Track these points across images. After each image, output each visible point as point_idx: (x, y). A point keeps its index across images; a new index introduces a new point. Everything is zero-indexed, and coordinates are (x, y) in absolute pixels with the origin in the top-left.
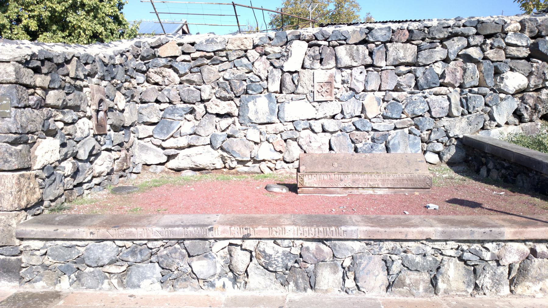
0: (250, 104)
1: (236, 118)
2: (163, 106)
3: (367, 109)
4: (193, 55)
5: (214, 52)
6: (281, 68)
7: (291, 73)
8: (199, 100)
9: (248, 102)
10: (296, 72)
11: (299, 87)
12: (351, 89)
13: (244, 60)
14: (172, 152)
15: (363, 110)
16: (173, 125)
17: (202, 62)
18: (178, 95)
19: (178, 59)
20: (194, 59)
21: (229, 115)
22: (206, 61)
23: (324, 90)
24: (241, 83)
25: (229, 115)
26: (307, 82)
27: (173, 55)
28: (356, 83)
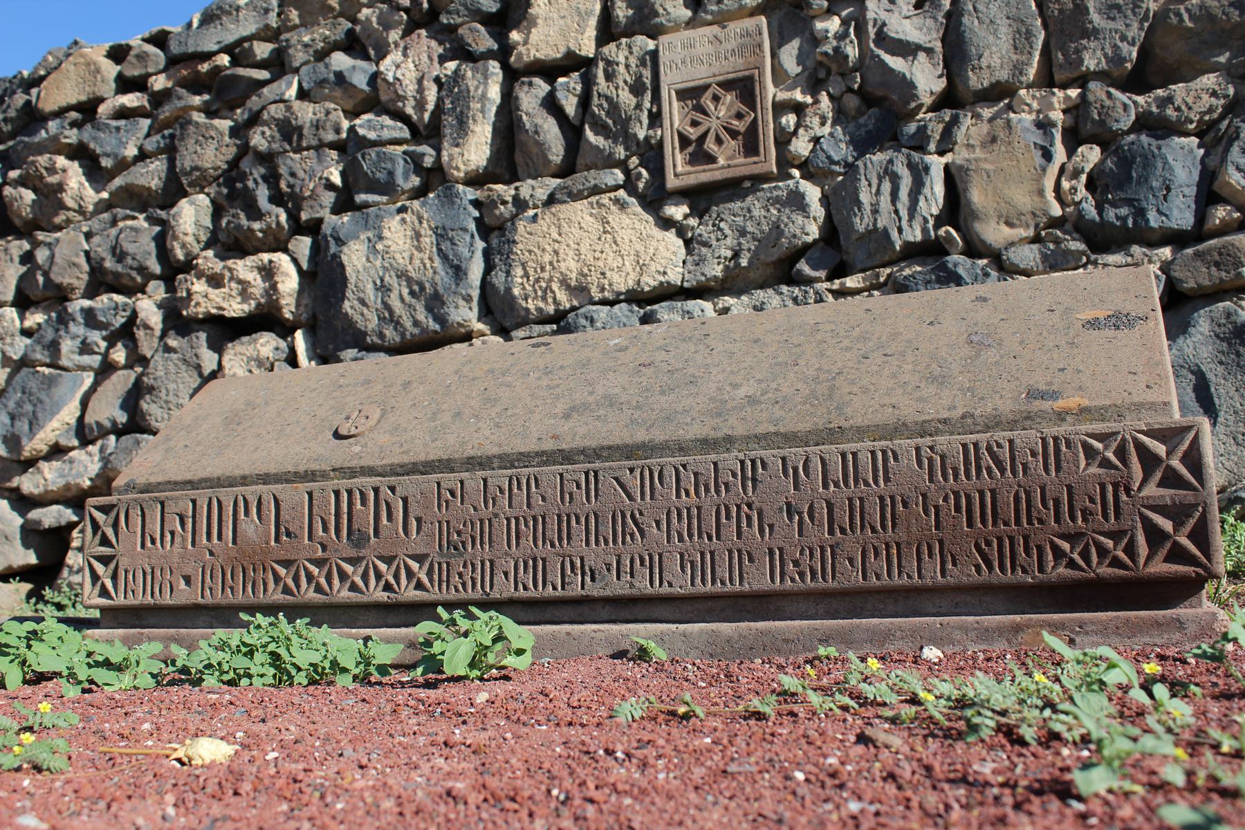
0: (354, 257)
1: (299, 335)
2: (36, 318)
3: (977, 196)
4: (159, 83)
5: (228, 50)
6: (504, 53)
7: (549, 71)
8: (157, 269)
9: (340, 242)
10: (572, 63)
11: (589, 134)
12: (867, 98)
13: (340, 60)
14: (51, 516)
15: (955, 208)
16: (59, 391)
17: (180, 104)
18: (82, 261)
19: (102, 109)
20: (159, 99)
21: (265, 319)
22: (197, 100)
23: (714, 124)
24: (320, 159)
25: (265, 319)
26: (626, 98)
27: (83, 98)
28: (896, 63)
